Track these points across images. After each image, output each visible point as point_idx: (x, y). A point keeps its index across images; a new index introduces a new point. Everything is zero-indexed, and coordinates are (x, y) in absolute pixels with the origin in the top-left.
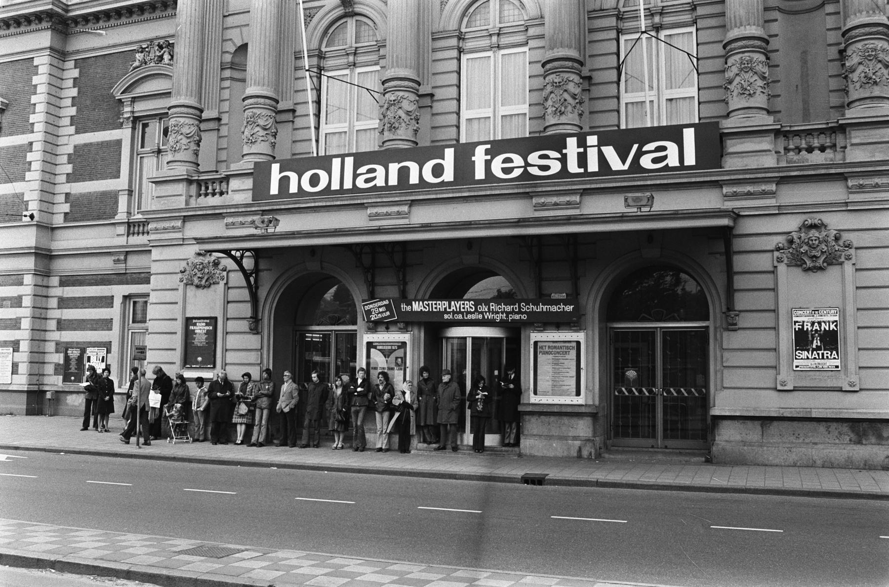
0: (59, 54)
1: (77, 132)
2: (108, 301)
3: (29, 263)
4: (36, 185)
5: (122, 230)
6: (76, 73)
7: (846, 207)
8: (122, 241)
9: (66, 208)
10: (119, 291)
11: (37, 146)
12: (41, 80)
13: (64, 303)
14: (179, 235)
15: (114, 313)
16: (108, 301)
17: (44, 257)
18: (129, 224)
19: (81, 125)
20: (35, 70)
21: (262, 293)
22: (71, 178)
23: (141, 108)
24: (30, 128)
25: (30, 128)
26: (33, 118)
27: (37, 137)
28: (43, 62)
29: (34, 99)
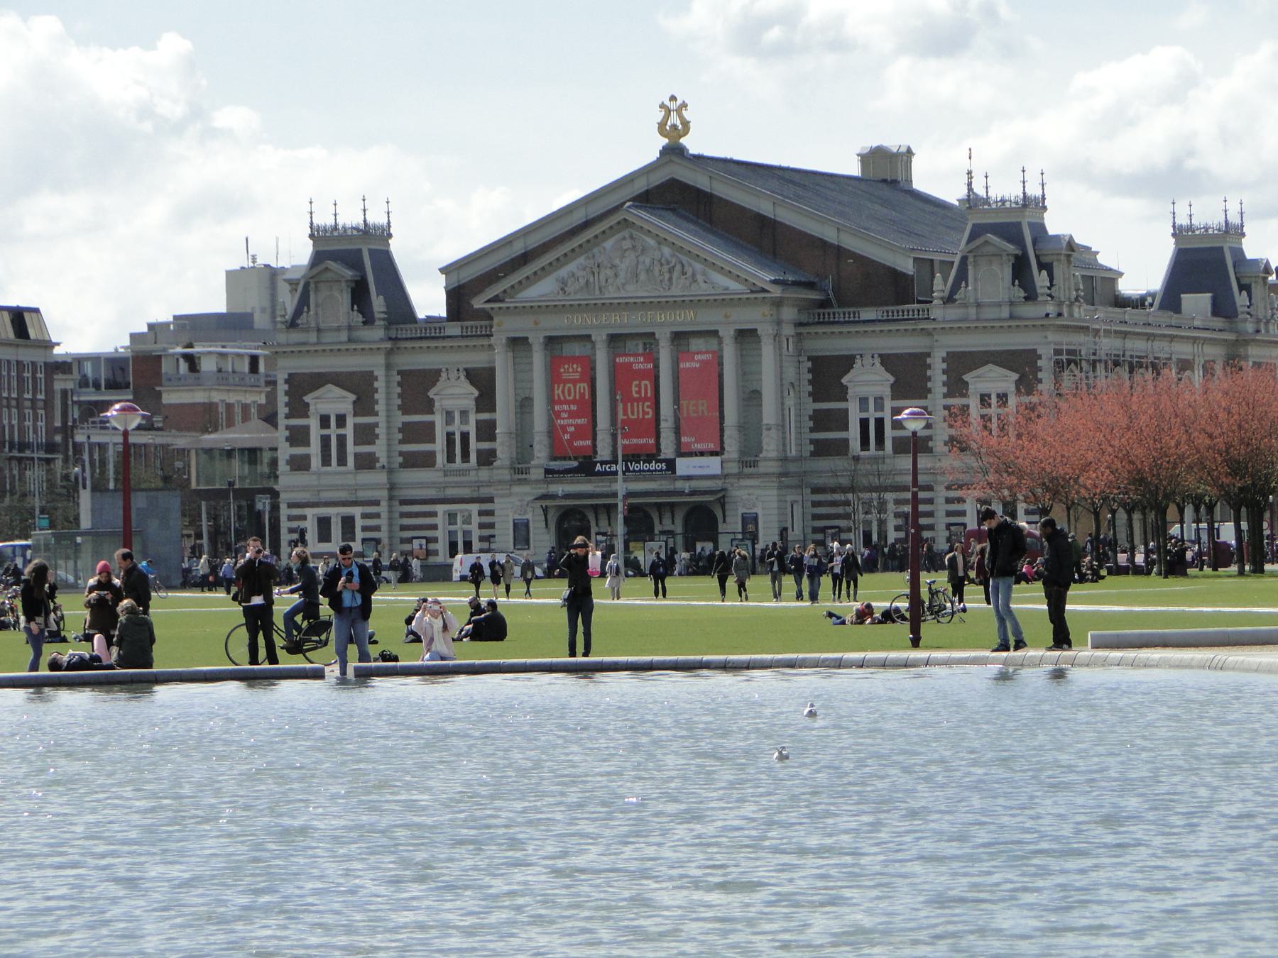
0: (388, 367)
2: (434, 514)
3: (385, 493)
4: (384, 448)
5: (441, 474)
6: (399, 378)
7: (758, 487)
8: (442, 479)
9: (401, 459)
10: (440, 509)
11: (383, 425)
12: (380, 384)
13: (403, 515)
15: (440, 521)
16: (434, 514)
19: (405, 409)
20: (376, 379)
21: (549, 517)
22: (401, 442)
24: (376, 414)
25: (376, 414)
26: (377, 408)
27: (381, 419)
28: (380, 373)
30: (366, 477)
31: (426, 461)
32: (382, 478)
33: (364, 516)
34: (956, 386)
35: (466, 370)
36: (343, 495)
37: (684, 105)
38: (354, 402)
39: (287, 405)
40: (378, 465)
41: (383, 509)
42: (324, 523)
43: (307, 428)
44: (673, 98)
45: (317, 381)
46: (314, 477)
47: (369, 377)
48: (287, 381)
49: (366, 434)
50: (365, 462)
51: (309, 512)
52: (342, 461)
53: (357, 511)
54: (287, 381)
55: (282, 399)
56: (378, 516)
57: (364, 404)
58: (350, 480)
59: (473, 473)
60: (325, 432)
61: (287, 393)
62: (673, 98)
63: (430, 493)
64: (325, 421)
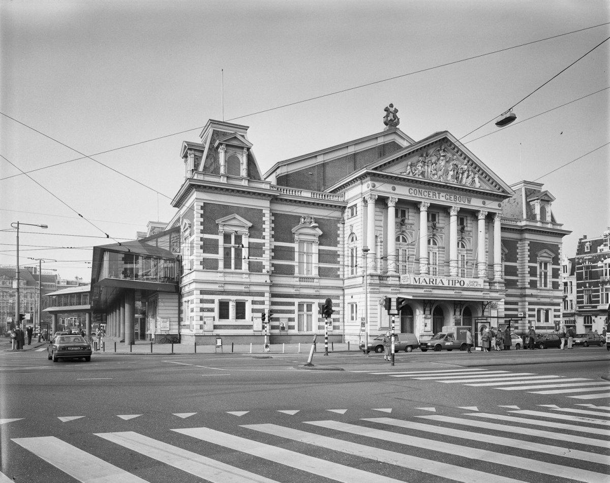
0: (271, 210)
1: (275, 241)
2: (293, 304)
5: (298, 279)
8: (298, 283)
10: (297, 301)
14: (378, 291)
15: (296, 308)
16: (293, 304)
17: (272, 285)
18: (300, 278)
23: (303, 237)
26: (264, 234)
28: (267, 212)
29: (264, 226)
30: (256, 278)
31: (289, 271)
32: (267, 279)
33: (254, 302)
34: (533, 259)
35: (314, 218)
36: (242, 288)
37: (396, 111)
38: (250, 228)
39: (202, 224)
40: (264, 271)
41: (267, 298)
42: (224, 306)
43: (217, 241)
44: (391, 106)
45: (226, 210)
46: (222, 274)
47: (260, 213)
48: (202, 208)
49: (255, 250)
50: (255, 268)
51: (217, 298)
52: (238, 266)
53: (249, 299)
54: (202, 208)
55: (197, 220)
56: (263, 303)
57: (255, 230)
58: (245, 279)
59: (315, 280)
60: (228, 245)
61: (202, 216)
62: (391, 106)
63: (292, 291)
64: (227, 237)
